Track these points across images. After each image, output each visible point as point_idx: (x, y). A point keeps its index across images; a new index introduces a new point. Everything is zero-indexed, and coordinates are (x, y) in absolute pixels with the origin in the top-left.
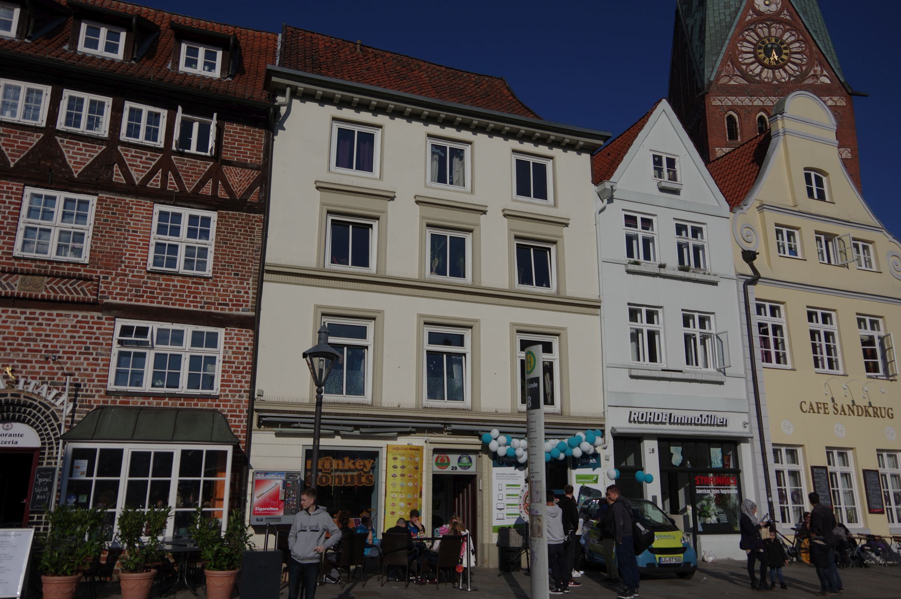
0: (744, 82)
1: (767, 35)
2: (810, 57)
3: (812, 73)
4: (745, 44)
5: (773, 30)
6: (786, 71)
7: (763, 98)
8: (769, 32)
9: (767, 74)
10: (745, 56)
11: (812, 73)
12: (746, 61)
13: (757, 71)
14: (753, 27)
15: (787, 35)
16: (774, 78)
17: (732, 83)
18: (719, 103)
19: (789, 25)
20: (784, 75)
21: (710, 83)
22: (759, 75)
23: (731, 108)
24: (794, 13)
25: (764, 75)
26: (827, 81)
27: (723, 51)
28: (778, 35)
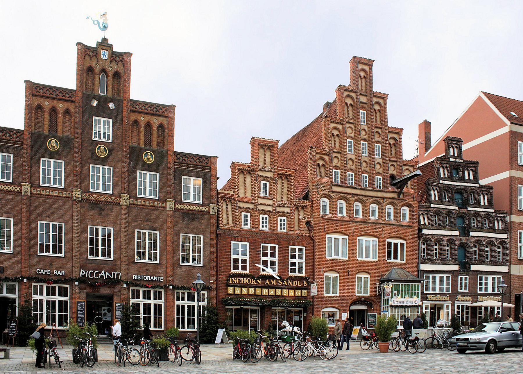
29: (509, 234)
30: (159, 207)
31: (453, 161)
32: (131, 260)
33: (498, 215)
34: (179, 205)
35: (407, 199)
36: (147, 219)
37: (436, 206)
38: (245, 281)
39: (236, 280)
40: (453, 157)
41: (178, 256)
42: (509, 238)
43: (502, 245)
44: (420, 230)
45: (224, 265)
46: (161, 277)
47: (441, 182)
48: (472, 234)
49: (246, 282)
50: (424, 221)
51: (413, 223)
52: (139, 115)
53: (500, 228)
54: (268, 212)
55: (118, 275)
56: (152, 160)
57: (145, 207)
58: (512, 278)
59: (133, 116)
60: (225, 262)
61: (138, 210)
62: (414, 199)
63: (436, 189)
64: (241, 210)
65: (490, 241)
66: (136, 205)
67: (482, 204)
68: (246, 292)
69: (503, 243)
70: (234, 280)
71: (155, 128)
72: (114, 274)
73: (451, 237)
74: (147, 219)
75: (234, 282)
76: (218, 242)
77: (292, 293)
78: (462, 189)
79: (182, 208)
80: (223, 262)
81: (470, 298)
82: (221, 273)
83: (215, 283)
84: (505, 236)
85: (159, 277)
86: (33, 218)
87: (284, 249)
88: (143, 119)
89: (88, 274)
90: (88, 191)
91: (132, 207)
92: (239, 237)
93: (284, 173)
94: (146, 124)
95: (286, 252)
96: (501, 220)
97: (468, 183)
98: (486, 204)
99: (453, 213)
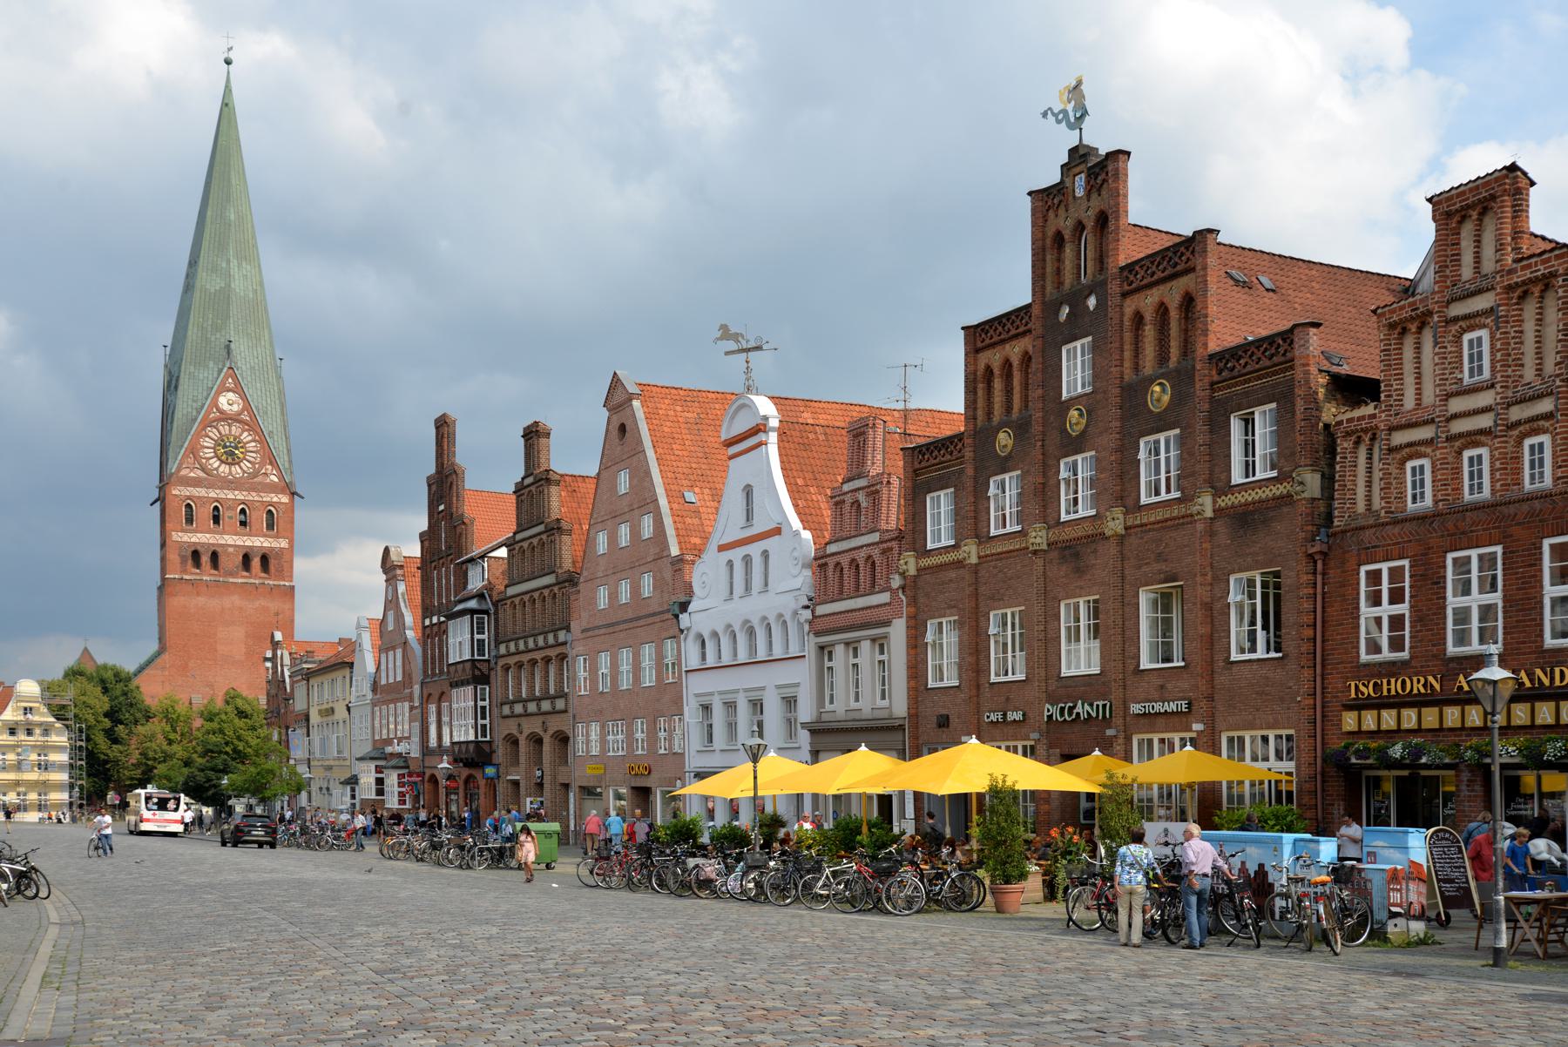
0: (202, 474)
1: (227, 432)
2: (263, 457)
3: (263, 471)
4: (207, 439)
5: (234, 428)
6: (241, 468)
7: (217, 491)
8: (230, 430)
9: (224, 469)
10: (206, 450)
11: (263, 471)
12: (208, 456)
13: (216, 465)
14: (215, 424)
15: (246, 434)
16: (230, 473)
17: (192, 475)
18: (178, 493)
19: (248, 425)
20: (239, 471)
21: (172, 474)
22: (217, 469)
23: (189, 498)
24: (253, 416)
25: (221, 469)
26: (276, 480)
27: (186, 445)
28: (237, 434)
30: (1183, 517)
32: (1132, 667)
34: (1223, 497)
36: (1160, 554)
38: (1393, 687)
39: (1367, 687)
41: (1224, 637)
45: (1341, 644)
46: (1183, 702)
49: (1396, 691)
52: (1141, 295)
54: (1475, 434)
55: (1104, 706)
56: (1166, 398)
57: (1156, 526)
59: (1129, 306)
60: (1342, 634)
61: (1142, 538)
64: (1398, 456)
66: (1137, 526)
68: (1392, 723)
70: (1362, 688)
71: (1174, 314)
72: (1098, 706)
74: (1160, 557)
75: (1363, 694)
76: (1319, 578)
77: (1476, 718)
79: (1230, 503)
80: (1337, 634)
82: (1332, 669)
83: (1312, 702)
85: (1179, 703)
86: (982, 609)
87: (1524, 556)
88: (1147, 302)
89: (1054, 710)
90: (1058, 523)
91: (1130, 535)
92: (1378, 546)
93: (1528, 274)
94: (1157, 312)
95: (1531, 565)
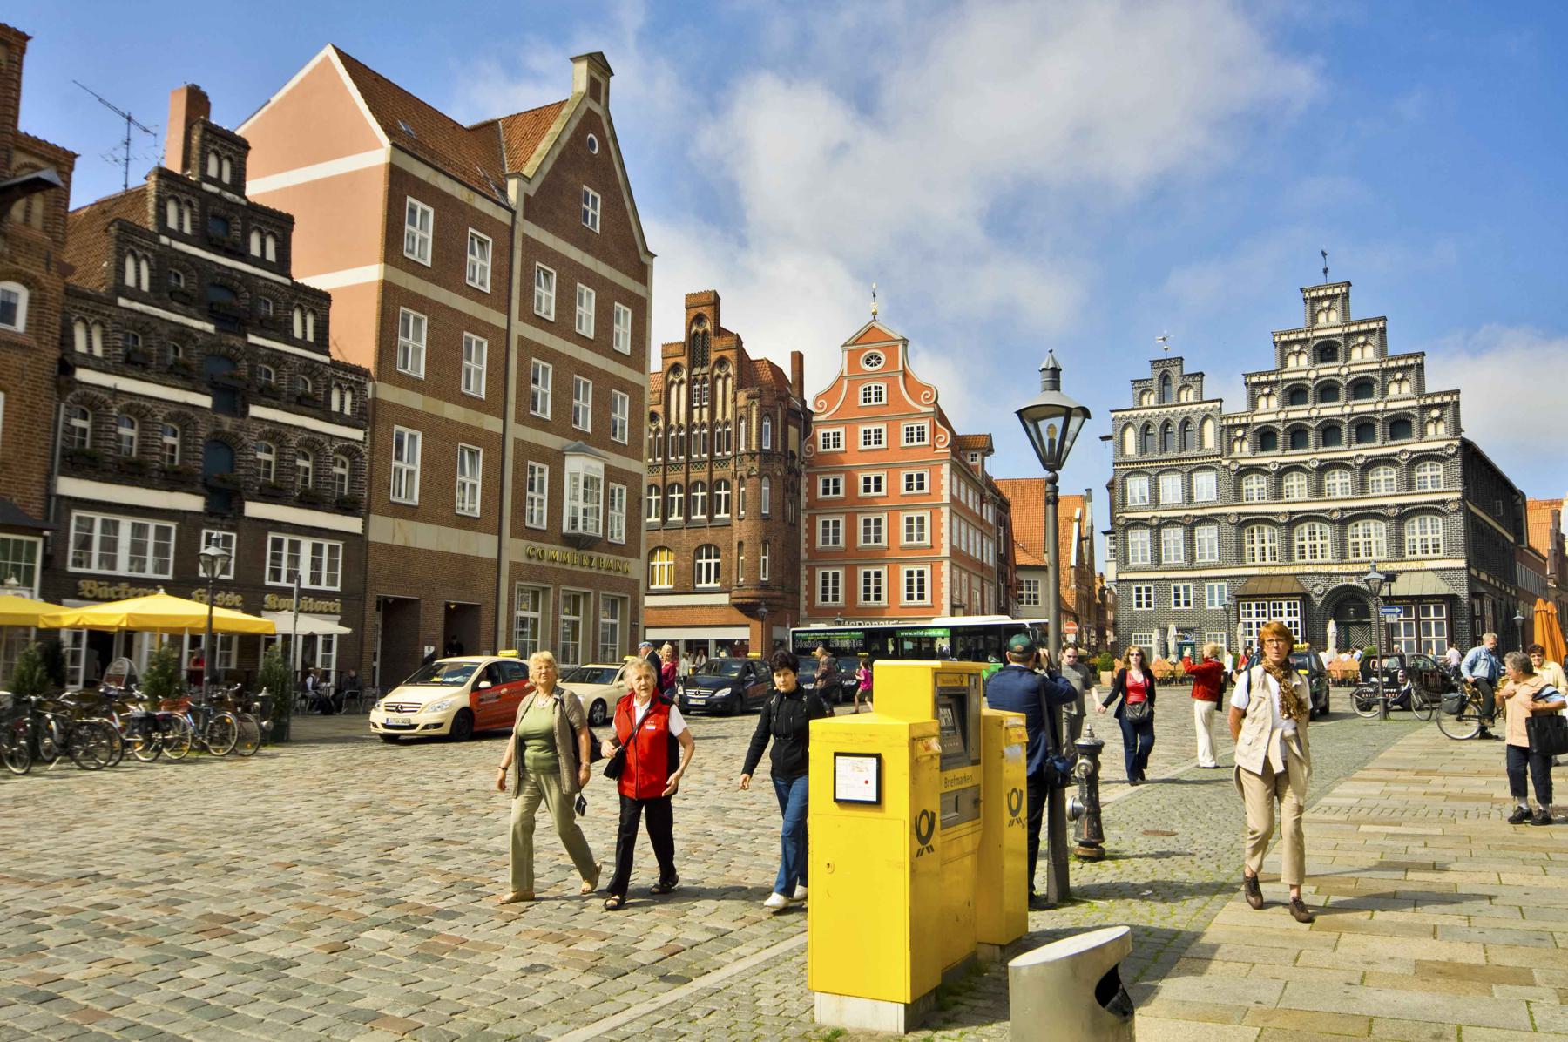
29: (369, 430)
31: (212, 194)
33: (341, 374)
35: (20, 260)
37: (137, 306)
40: (217, 182)
42: (368, 441)
43: (349, 456)
44: (66, 367)
47: (164, 240)
48: (256, 411)
50: (90, 344)
51: (38, 340)
53: (347, 411)
58: (371, 550)
62: (48, 264)
63: (146, 257)
65: (313, 440)
67: (298, 334)
69: (350, 450)
73: (183, 410)
78: (235, 279)
81: (237, 599)
84: (358, 434)
96: (350, 388)
97: (255, 265)
98: (310, 338)
99: (195, 340)
